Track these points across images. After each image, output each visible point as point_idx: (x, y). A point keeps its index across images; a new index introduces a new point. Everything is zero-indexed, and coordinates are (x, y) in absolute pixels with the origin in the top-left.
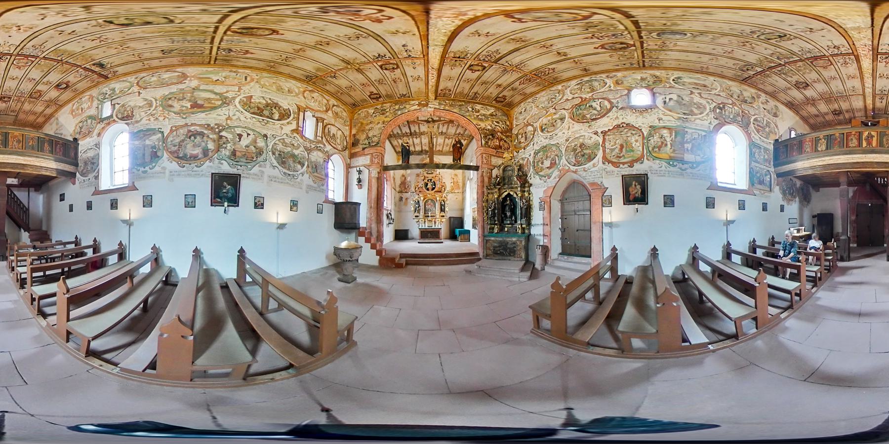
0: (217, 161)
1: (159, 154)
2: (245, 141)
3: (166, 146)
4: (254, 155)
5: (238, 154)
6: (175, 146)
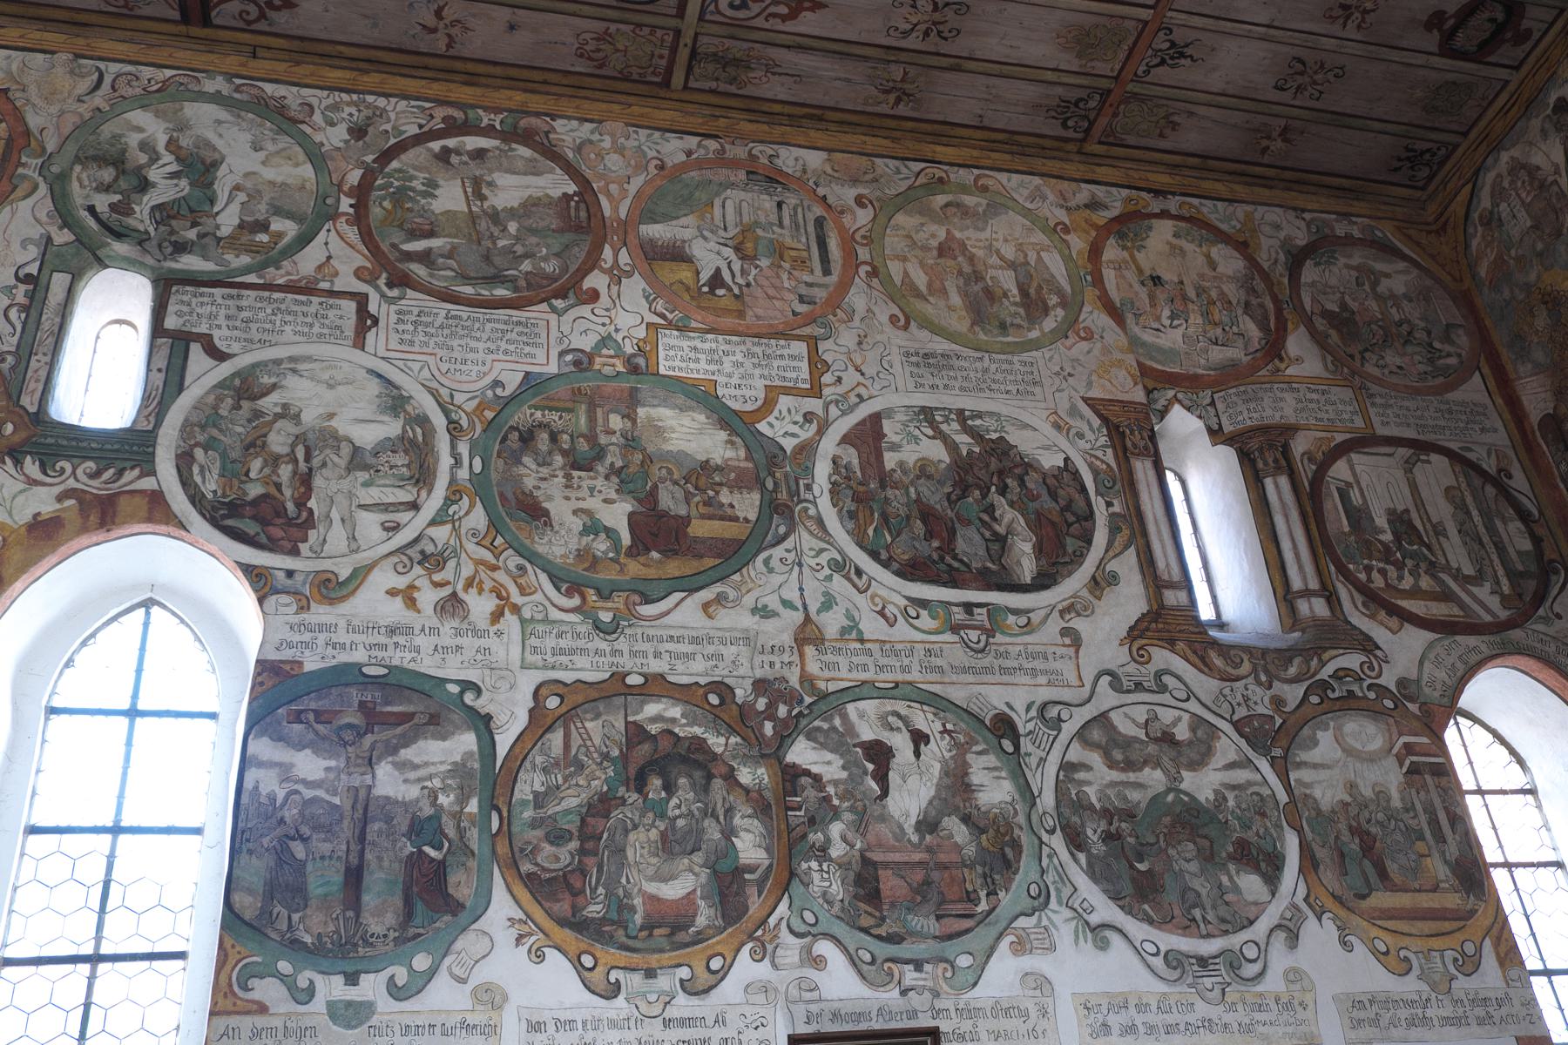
0: (790, 948)
1: (461, 885)
2: (910, 797)
3: (507, 822)
4: (973, 880)
5: (890, 884)
6: (557, 837)
